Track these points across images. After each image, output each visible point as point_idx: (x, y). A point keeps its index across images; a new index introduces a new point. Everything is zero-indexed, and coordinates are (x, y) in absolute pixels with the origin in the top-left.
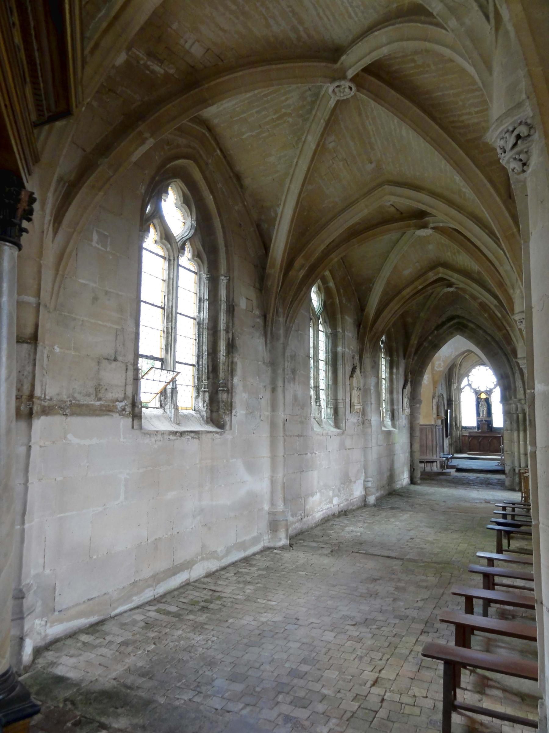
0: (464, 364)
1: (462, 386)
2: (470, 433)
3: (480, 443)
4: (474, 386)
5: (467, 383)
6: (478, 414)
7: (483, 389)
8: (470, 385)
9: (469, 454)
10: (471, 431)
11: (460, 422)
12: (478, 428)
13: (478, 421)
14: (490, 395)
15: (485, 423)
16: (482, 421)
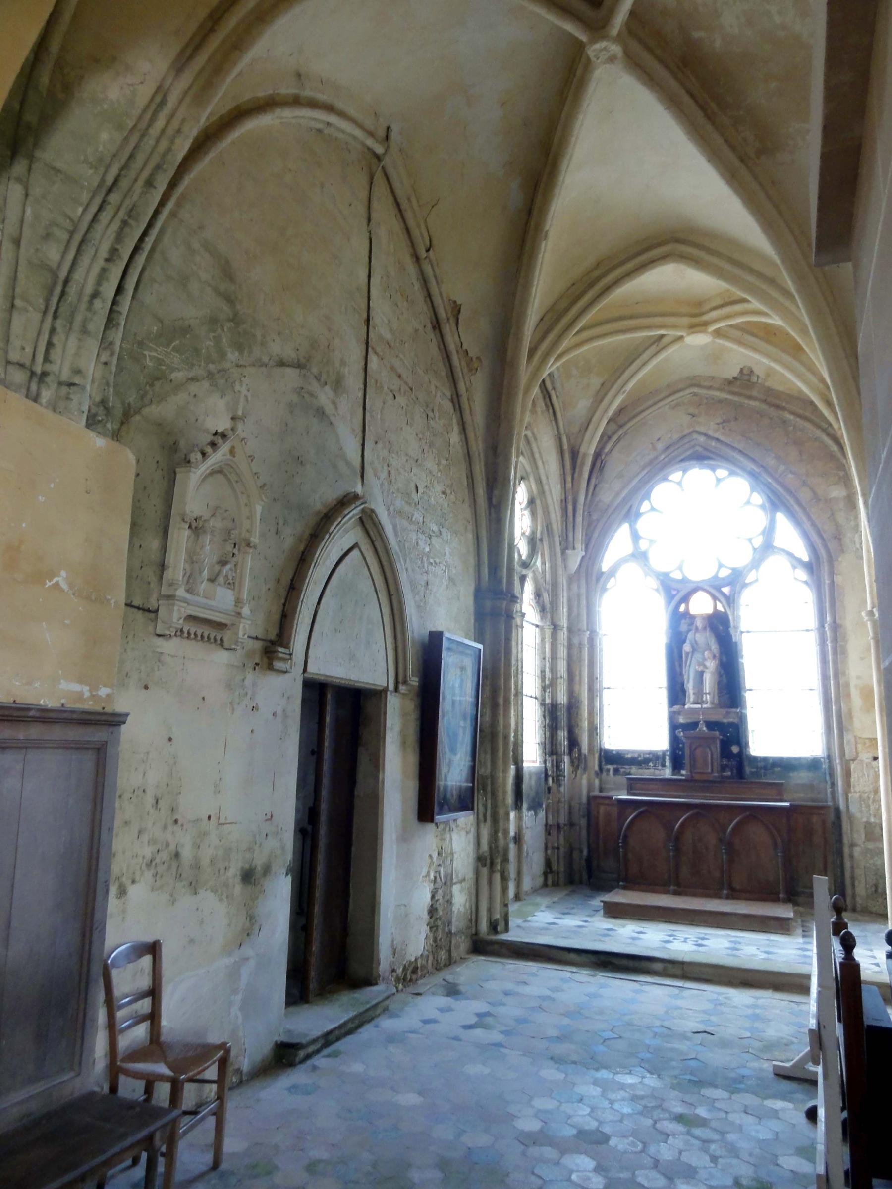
0: (615, 463)
1: (606, 563)
2: (633, 785)
3: (678, 839)
4: (661, 562)
5: (629, 549)
6: (677, 693)
7: (699, 571)
8: (640, 556)
9: (614, 911)
10: (646, 774)
11: (594, 731)
12: (677, 765)
13: (674, 727)
14: (731, 601)
15: (712, 739)
16: (695, 725)
